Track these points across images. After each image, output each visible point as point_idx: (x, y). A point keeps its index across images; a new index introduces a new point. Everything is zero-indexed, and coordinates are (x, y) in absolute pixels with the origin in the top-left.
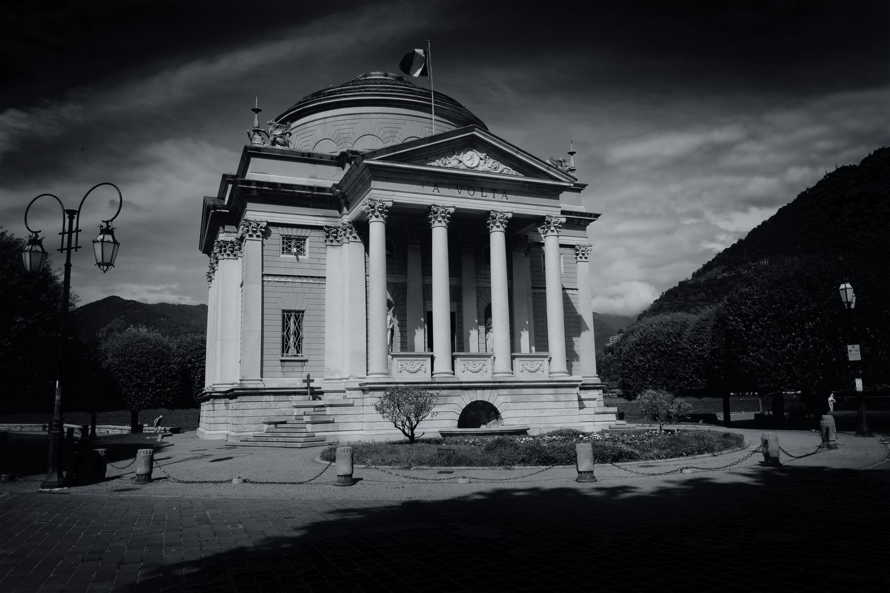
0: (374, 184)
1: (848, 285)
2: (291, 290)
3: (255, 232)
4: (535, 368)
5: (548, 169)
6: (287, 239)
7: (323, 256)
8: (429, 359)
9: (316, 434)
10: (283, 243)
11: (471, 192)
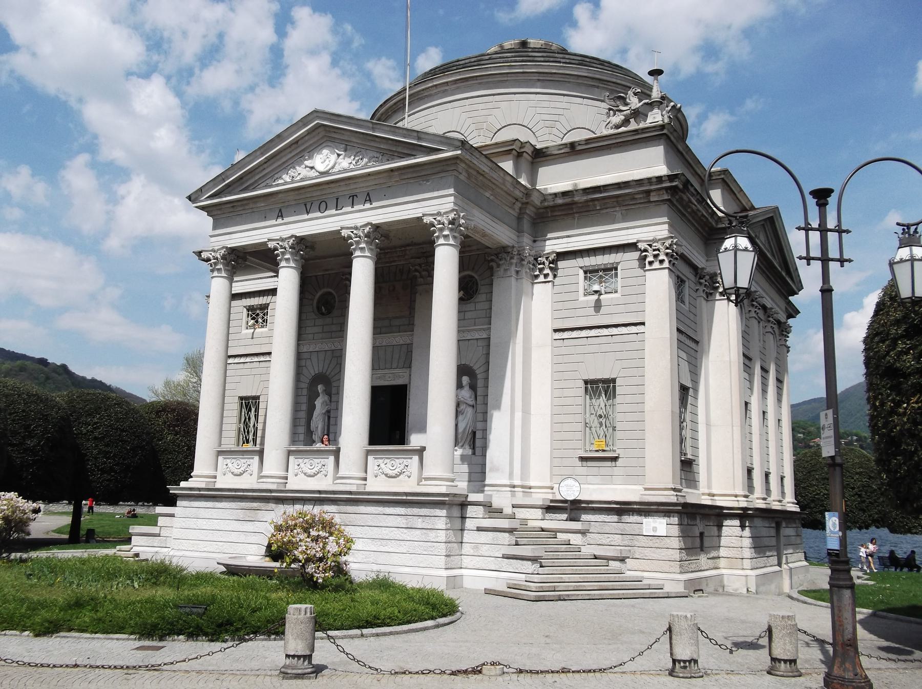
1: (743, 242)
5: (419, 139)
6: (250, 309)
8: (257, 458)
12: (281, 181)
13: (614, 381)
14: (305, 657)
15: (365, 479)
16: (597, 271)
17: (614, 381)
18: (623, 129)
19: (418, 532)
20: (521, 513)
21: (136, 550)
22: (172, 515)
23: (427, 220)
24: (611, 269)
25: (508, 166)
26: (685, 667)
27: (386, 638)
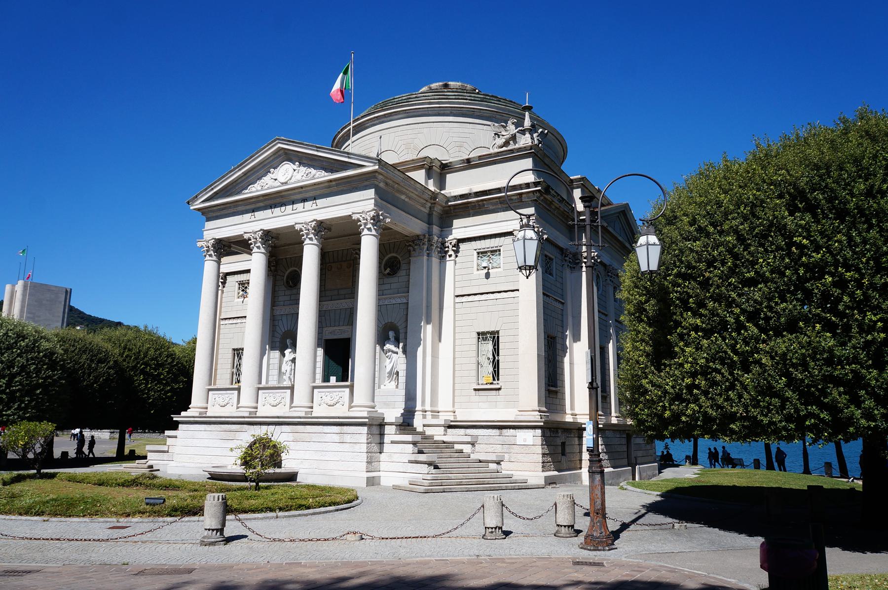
0: (209, 225)
4: (335, 400)
11: (283, 208)
12: (254, 189)
13: (498, 332)
14: (217, 530)
15: (312, 408)
16: (486, 252)
17: (498, 332)
18: (504, 149)
20: (429, 431)
21: (150, 463)
22: (176, 437)
23: (355, 217)
24: (495, 252)
25: (419, 176)
26: (492, 532)
27: (295, 519)
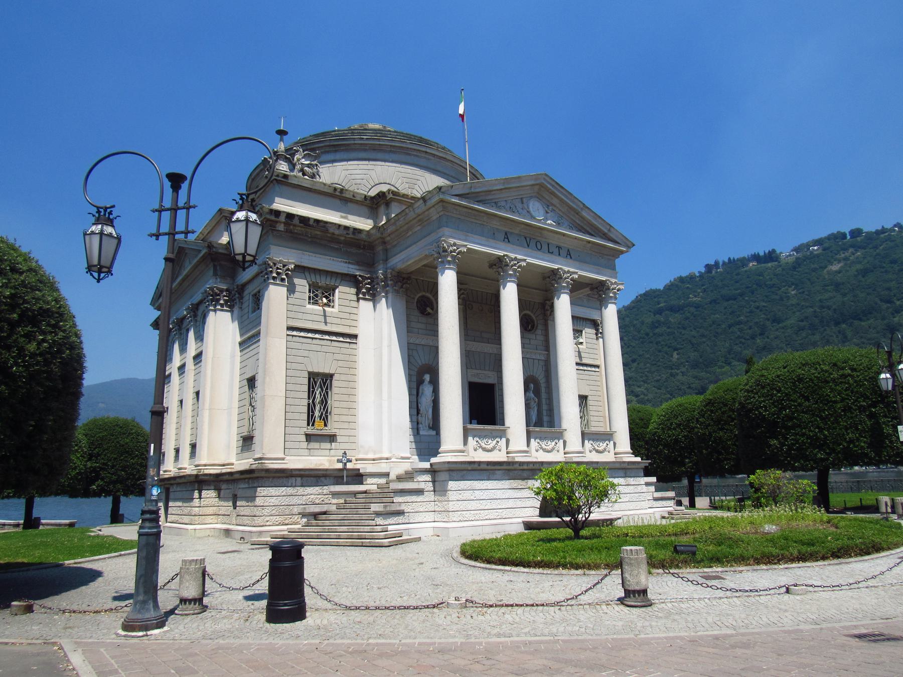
2: (318, 348)
3: (278, 274)
7: (354, 311)
9: (390, 528)
10: (310, 292)
19: (632, 487)
